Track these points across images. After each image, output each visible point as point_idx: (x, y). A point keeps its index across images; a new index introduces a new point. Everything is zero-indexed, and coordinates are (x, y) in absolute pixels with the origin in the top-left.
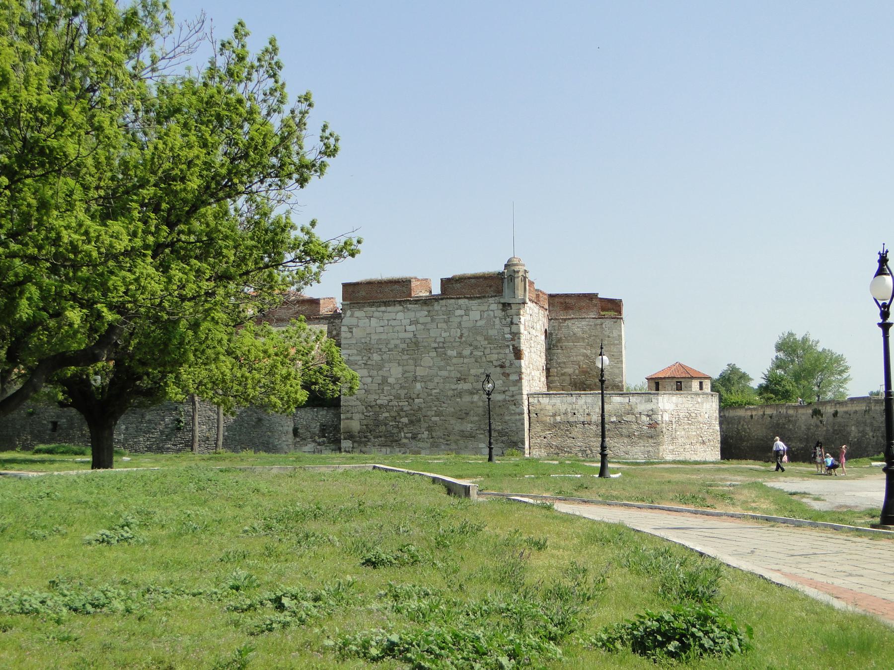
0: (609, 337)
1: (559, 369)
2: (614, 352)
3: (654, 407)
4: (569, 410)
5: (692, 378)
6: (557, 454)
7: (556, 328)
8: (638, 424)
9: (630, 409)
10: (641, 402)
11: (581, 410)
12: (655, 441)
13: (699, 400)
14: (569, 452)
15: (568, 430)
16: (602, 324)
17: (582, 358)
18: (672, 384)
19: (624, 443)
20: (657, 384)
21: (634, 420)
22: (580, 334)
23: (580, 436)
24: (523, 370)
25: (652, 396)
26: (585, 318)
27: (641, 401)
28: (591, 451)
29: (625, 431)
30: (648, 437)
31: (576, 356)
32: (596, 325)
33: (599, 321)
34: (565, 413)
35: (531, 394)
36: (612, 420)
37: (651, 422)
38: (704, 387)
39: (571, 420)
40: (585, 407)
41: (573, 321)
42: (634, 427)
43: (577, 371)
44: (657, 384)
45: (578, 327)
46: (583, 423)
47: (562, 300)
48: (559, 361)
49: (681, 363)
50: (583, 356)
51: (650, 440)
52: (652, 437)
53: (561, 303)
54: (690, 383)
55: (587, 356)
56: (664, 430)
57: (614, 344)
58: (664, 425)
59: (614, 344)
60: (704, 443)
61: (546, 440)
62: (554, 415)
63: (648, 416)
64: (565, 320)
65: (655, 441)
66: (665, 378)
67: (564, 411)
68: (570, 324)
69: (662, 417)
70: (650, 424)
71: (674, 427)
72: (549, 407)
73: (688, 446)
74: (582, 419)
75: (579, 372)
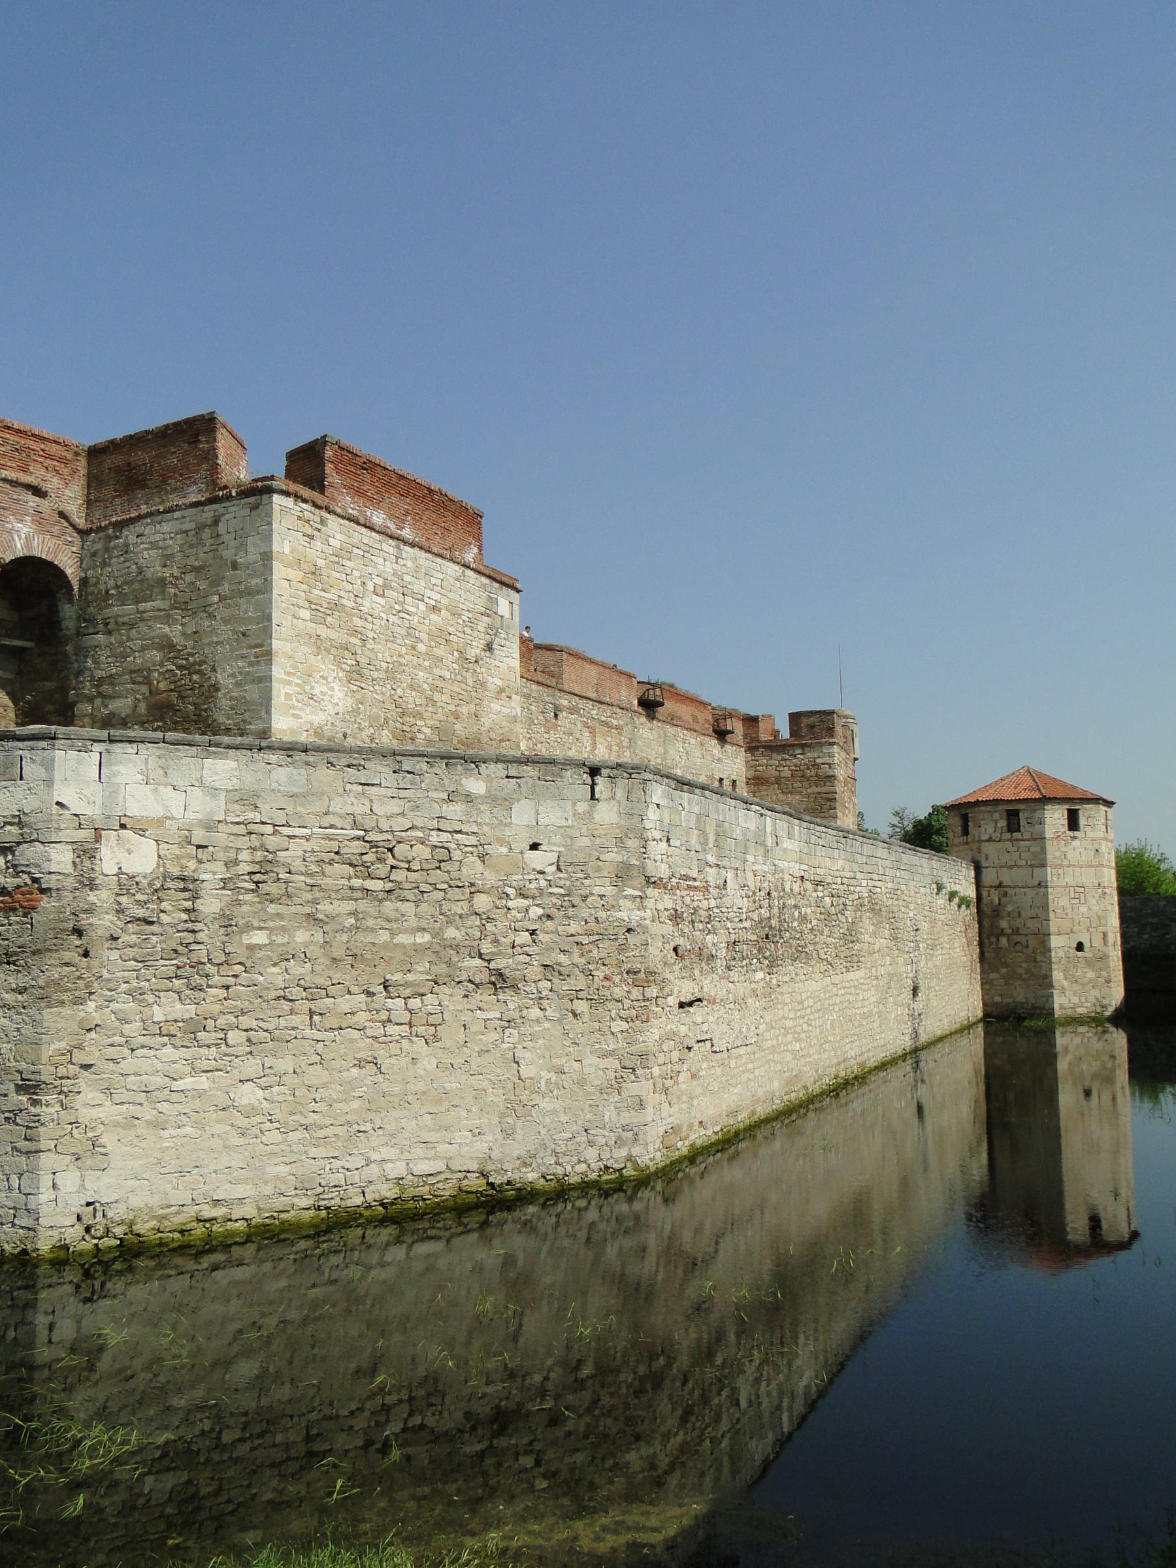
0: (235, 566)
1: (98, 702)
2: (250, 620)
3: (30, 804)
5: (1045, 800)
12: (22, 980)
13: (476, 786)
16: (216, 522)
17: (157, 656)
18: (996, 816)
20: (965, 819)
22: (155, 570)
25: (20, 749)
26: (170, 510)
31: (143, 649)
32: (200, 528)
33: (208, 513)
38: (1082, 821)
41: (138, 528)
43: (142, 708)
44: (965, 819)
45: (154, 545)
48: (99, 673)
49: (1033, 767)
50: (161, 648)
53: (118, 470)
54: (1038, 814)
55: (172, 647)
56: (103, 922)
57: (250, 593)
58: (102, 897)
59: (250, 593)
60: (499, 981)
64: (120, 525)
65: (22, 980)
66: (978, 803)
68: (132, 539)
69: (86, 853)
71: (210, 904)
73: (344, 1004)
75: (150, 708)
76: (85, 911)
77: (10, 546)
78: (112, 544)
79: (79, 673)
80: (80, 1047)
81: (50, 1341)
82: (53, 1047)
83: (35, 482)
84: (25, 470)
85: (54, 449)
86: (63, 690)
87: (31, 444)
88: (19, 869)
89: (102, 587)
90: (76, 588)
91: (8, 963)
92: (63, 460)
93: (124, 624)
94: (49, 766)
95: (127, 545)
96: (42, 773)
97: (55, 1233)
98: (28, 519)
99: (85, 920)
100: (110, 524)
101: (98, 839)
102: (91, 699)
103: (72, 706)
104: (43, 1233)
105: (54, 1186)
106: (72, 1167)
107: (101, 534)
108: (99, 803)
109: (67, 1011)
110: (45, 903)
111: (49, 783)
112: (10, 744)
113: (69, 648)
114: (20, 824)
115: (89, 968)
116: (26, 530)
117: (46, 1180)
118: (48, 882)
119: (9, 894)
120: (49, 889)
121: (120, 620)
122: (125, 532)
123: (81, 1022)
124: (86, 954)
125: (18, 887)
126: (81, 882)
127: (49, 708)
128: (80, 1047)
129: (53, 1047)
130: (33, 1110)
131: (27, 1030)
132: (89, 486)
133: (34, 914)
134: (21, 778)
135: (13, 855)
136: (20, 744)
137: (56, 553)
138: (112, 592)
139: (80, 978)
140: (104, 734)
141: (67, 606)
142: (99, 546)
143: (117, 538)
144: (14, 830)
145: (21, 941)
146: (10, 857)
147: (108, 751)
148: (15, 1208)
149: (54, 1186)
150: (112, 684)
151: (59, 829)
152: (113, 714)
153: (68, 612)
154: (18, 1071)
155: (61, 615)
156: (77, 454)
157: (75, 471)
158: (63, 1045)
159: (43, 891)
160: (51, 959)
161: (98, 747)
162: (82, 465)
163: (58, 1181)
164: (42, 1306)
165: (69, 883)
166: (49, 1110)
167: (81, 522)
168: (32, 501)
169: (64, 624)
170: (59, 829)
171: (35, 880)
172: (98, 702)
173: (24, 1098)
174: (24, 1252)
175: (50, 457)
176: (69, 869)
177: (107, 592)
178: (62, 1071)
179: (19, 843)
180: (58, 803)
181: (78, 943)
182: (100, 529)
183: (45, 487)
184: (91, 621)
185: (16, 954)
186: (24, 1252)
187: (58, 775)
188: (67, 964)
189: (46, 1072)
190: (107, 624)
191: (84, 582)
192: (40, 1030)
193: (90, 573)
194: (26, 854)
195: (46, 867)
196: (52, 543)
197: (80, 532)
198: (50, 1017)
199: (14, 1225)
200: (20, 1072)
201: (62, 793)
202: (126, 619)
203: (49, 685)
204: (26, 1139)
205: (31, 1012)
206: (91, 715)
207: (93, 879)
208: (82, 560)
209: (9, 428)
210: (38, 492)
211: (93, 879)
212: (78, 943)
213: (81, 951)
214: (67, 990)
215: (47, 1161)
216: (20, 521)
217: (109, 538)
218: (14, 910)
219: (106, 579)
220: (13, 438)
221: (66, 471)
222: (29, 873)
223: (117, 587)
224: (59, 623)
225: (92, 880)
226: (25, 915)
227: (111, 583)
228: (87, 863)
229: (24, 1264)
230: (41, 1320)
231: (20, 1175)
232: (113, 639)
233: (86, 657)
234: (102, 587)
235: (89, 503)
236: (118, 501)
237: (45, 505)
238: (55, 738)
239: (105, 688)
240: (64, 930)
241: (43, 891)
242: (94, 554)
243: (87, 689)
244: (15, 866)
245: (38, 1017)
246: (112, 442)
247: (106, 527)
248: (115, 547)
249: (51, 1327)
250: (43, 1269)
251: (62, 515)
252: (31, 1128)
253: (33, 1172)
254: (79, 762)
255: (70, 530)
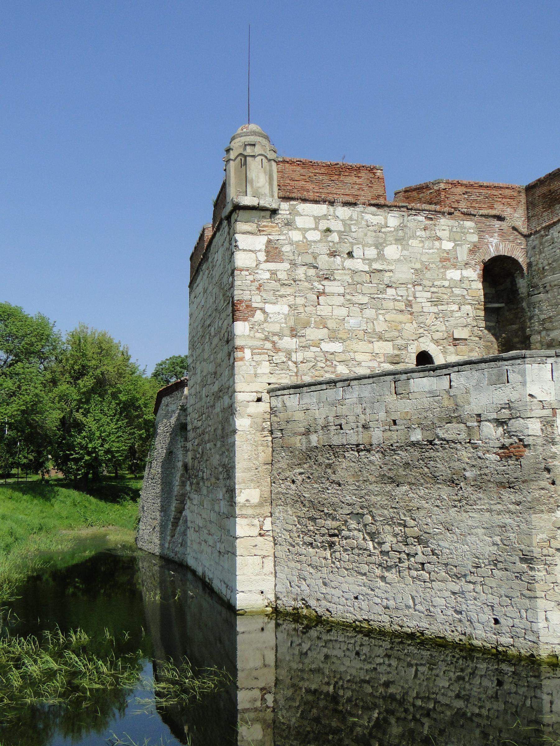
1: (544, 333)
3: (514, 396)
4: (331, 419)
6: (313, 519)
7: (537, 250)
8: (475, 447)
9: (452, 406)
10: (478, 386)
11: (352, 419)
14: (334, 519)
15: (329, 466)
19: (440, 498)
21: (463, 436)
23: (351, 481)
24: (238, 342)
25: (506, 366)
27: (479, 381)
28: (373, 517)
29: (443, 470)
30: (501, 485)
34: (325, 427)
35: (273, 390)
36: (413, 439)
37: (507, 442)
39: (336, 440)
40: (359, 410)
42: (465, 454)
46: (357, 448)
47: (544, 190)
48: (543, 317)
51: (507, 495)
52: (510, 486)
53: (544, 196)
61: (293, 486)
62: (307, 433)
63: (500, 423)
67: (321, 422)
70: (503, 447)
72: (299, 416)
74: (354, 439)
76: (551, 457)
77: (488, 252)
78: (544, 240)
79: (531, 318)
80: (554, 538)
81: (551, 711)
82: (539, 537)
83: (498, 213)
84: (492, 208)
85: (507, 192)
86: (523, 329)
87: (495, 192)
88: (511, 434)
89: (541, 266)
90: (525, 269)
91: (510, 487)
92: (512, 198)
93: (555, 285)
94: (523, 373)
95: (553, 239)
96: (520, 378)
97: (549, 647)
98: (496, 234)
99: (552, 463)
100: (542, 228)
101: (555, 415)
102: (539, 333)
103: (528, 337)
104: (542, 645)
105: (546, 619)
106: (555, 609)
107: (538, 235)
108: (553, 393)
109: (545, 516)
110: (527, 453)
111: (524, 383)
112: (501, 363)
113: (524, 304)
114: (510, 408)
115: (555, 491)
116: (495, 241)
117: (541, 615)
118: (529, 441)
119: (507, 448)
120: (529, 445)
121: (553, 284)
122: (551, 231)
123: (554, 523)
124: (553, 483)
125: (512, 444)
126: (547, 441)
127: (516, 340)
128: (554, 538)
129: (539, 537)
130: (530, 573)
131: (523, 526)
132: (528, 209)
133: (522, 460)
134: (508, 382)
135: (507, 426)
136: (506, 363)
137: (512, 251)
138: (546, 268)
139: (551, 497)
140: (552, 352)
141: (521, 280)
142: (537, 242)
143: (547, 235)
144: (506, 411)
145: (515, 475)
146: (505, 427)
147: (556, 362)
148: (524, 629)
149: (546, 619)
150: (551, 322)
151: (531, 410)
152: (553, 340)
153: (522, 284)
154: (520, 550)
155: (518, 286)
156: (519, 192)
157: (519, 202)
158: (544, 536)
159: (525, 446)
160: (534, 485)
161: (550, 360)
162: (523, 198)
163: (548, 616)
164: (545, 690)
165: (540, 441)
166: (540, 574)
167: (525, 231)
168: (497, 224)
169: (521, 291)
170: (531, 410)
171: (521, 440)
172: (544, 333)
173: (525, 566)
174: (532, 655)
175: (505, 197)
176: (539, 433)
177: (543, 268)
178: (545, 552)
179: (510, 419)
180: (530, 395)
181: (548, 476)
182: (537, 232)
183: (504, 214)
184: (535, 287)
185: (513, 482)
186: (532, 655)
187: (528, 379)
188: (543, 489)
189: (537, 551)
190: (545, 287)
191: (530, 265)
192: (530, 527)
193: (532, 259)
194: (515, 425)
195: (526, 432)
196: (510, 246)
197: (526, 236)
198: (535, 518)
199: (525, 639)
200: (522, 551)
201: (532, 389)
202: (556, 283)
203: (515, 327)
204: (528, 590)
205: (525, 516)
206: (541, 342)
207: (554, 439)
208: (527, 252)
209: (481, 186)
210: (500, 218)
211: (554, 439)
212: (548, 476)
213: (550, 481)
214: (544, 504)
215: (541, 603)
216: (492, 237)
217: (542, 236)
218: (511, 457)
219: (542, 261)
220: (484, 191)
221: (514, 203)
222: (517, 436)
223: (549, 264)
224: (517, 290)
225: (553, 439)
226: (517, 460)
227: (546, 262)
228: (549, 429)
229: (533, 662)
230: (546, 698)
231: (527, 610)
232: (549, 296)
233: (534, 308)
234: (541, 266)
235: (529, 219)
236: (545, 214)
237: (504, 225)
238: (524, 358)
239: (547, 325)
240: (539, 469)
241: (525, 446)
242: (534, 248)
243: (537, 327)
244: (509, 432)
245: (529, 519)
246: (539, 180)
247: (540, 231)
248: (546, 241)
249: (551, 703)
250: (544, 668)
251: (514, 229)
252: (530, 583)
253: (534, 609)
254: (540, 370)
255: (519, 236)
